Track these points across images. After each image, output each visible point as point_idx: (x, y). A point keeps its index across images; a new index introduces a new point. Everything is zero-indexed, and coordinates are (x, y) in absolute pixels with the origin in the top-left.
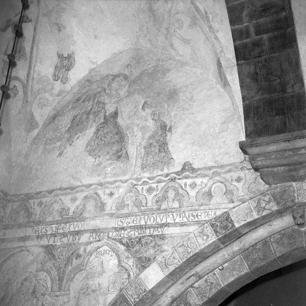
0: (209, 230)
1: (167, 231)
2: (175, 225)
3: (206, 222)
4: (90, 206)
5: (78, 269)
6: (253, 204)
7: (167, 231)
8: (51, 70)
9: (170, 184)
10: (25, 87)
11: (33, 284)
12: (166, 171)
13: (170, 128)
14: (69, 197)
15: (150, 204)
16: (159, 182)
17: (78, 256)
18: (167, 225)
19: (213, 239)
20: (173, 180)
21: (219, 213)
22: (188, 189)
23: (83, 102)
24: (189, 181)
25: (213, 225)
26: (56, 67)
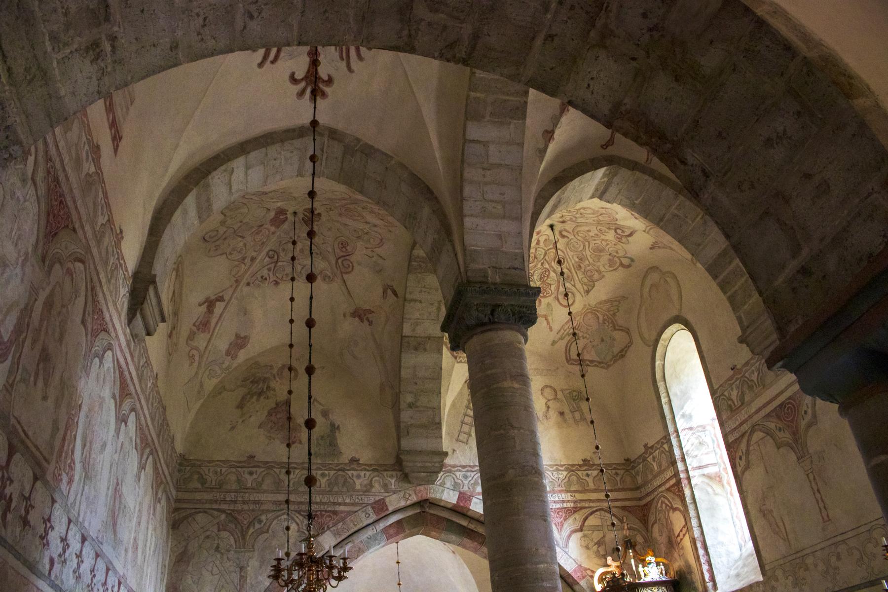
0: (370, 510)
1: (338, 508)
2: (345, 504)
3: (368, 504)
4: (268, 481)
5: (261, 532)
6: (402, 494)
7: (338, 508)
8: (227, 347)
9: (340, 473)
10: (201, 357)
11: (216, 542)
12: (336, 462)
13: (338, 427)
14: (246, 470)
15: (323, 486)
16: (330, 469)
17: (260, 522)
18: (340, 504)
19: (373, 517)
20: (343, 470)
21: (377, 498)
22: (355, 479)
23: (252, 382)
24: (355, 473)
25: (373, 508)
26: (231, 344)
